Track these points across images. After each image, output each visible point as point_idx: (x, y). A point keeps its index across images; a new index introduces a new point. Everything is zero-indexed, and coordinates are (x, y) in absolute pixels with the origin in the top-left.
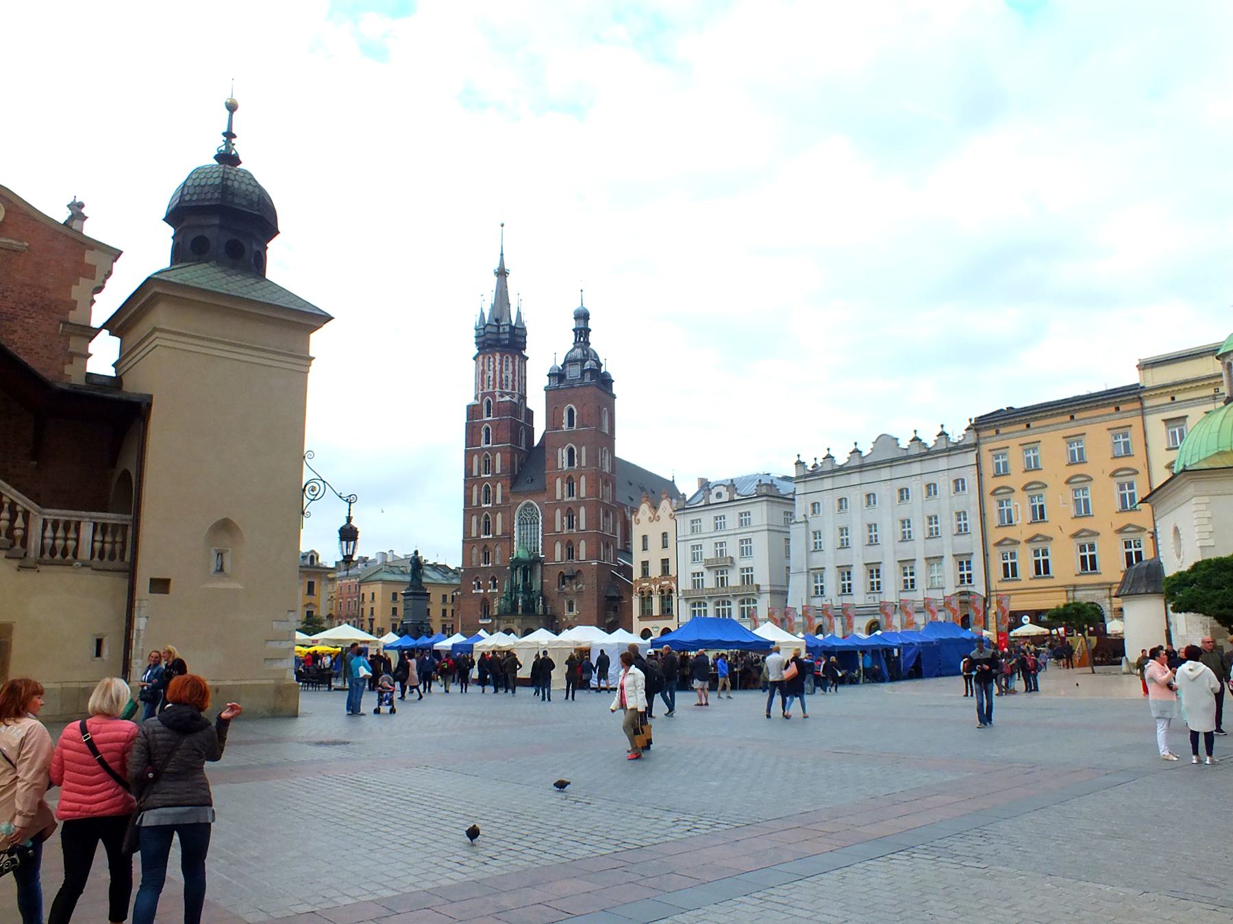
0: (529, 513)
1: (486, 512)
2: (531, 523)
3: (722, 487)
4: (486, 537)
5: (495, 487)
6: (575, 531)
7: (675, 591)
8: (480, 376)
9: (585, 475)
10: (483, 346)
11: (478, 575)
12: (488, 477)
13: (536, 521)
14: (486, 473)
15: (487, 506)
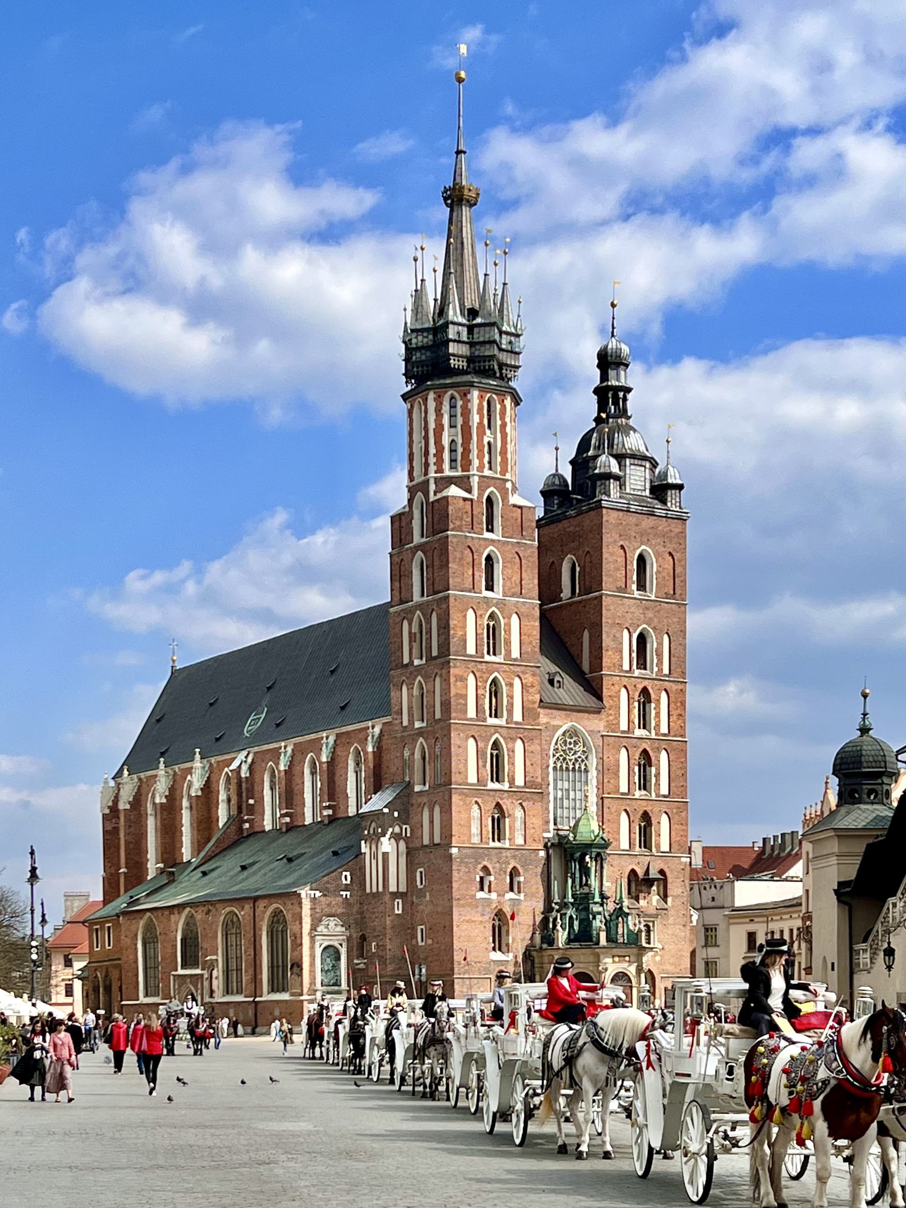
0: (569, 749)
1: (497, 735)
5: (511, 685)
11: (485, 863)
13: (583, 767)
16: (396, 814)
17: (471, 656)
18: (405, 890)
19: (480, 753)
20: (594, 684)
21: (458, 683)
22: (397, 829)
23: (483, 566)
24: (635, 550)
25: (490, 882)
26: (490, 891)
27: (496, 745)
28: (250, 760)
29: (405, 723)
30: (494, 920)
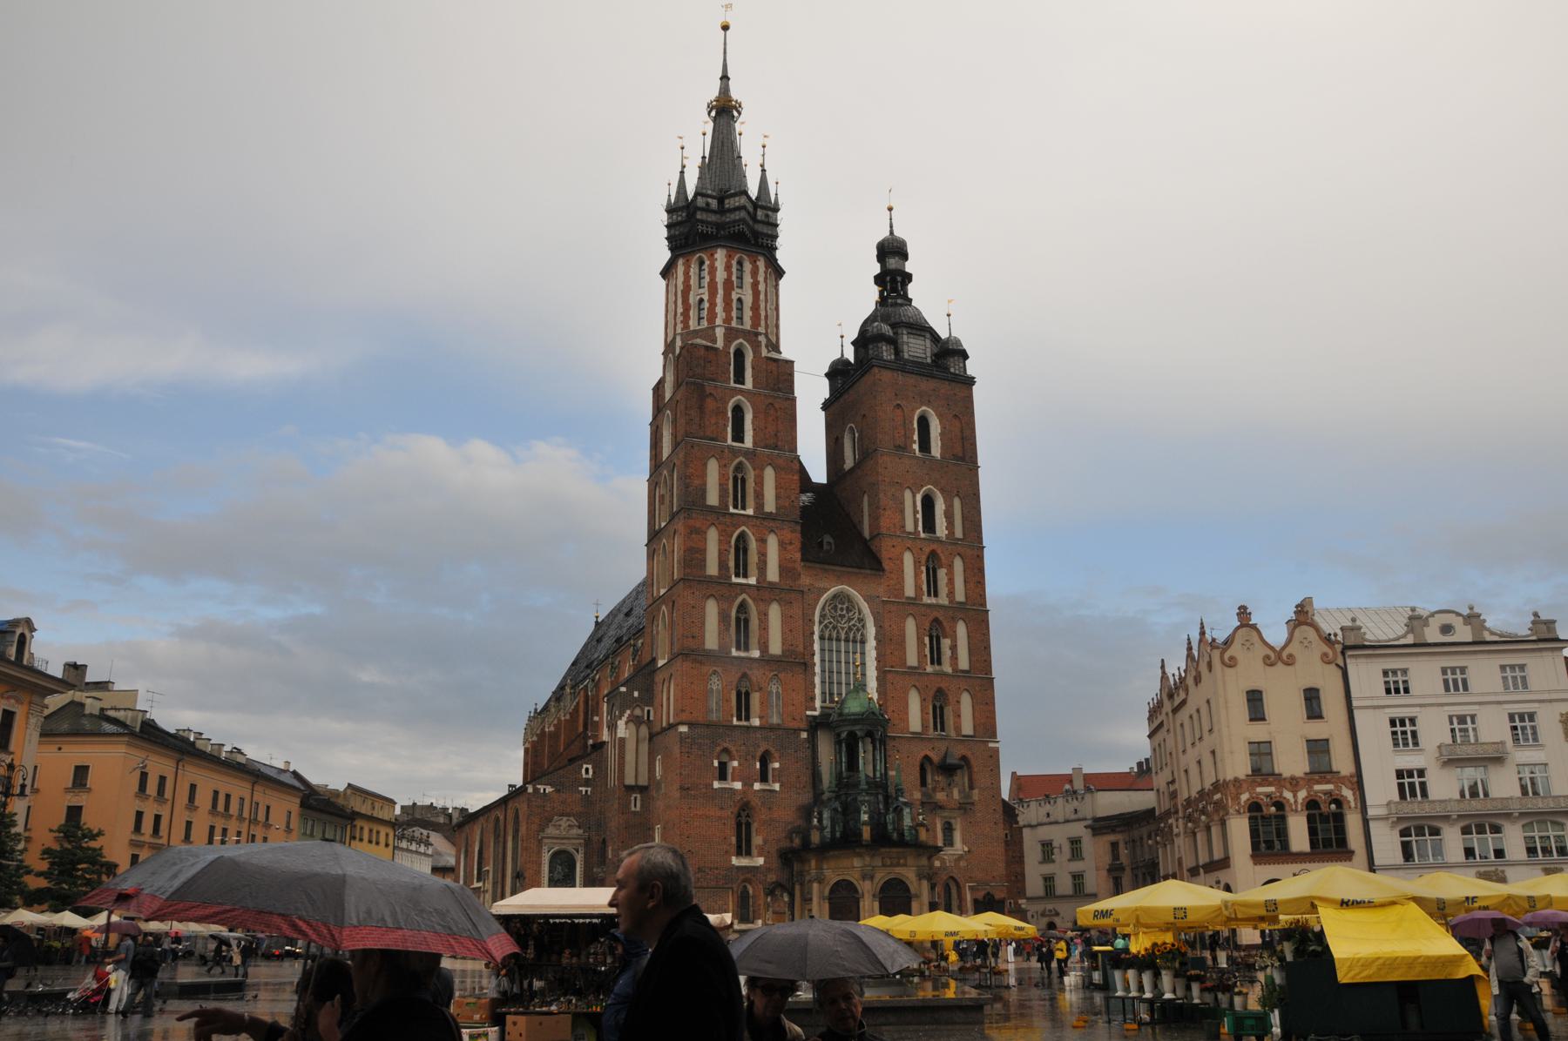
0: (840, 615)
1: (744, 596)
2: (847, 640)
3: (1454, 615)
4: (743, 654)
5: (762, 541)
6: (947, 668)
7: (1353, 804)
8: (721, 292)
9: (962, 558)
10: (717, 233)
11: (726, 745)
12: (748, 516)
13: (859, 638)
14: (735, 507)
15: (741, 580)
16: (636, 694)
17: (712, 507)
18: (646, 784)
19: (723, 617)
20: (873, 548)
21: (693, 536)
22: (638, 712)
23: (730, 414)
24: (913, 411)
25: (734, 768)
26: (733, 780)
27: (743, 607)
28: (597, 677)
29: (655, 595)
30: (739, 815)
